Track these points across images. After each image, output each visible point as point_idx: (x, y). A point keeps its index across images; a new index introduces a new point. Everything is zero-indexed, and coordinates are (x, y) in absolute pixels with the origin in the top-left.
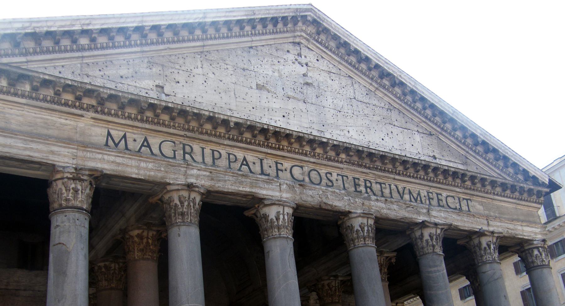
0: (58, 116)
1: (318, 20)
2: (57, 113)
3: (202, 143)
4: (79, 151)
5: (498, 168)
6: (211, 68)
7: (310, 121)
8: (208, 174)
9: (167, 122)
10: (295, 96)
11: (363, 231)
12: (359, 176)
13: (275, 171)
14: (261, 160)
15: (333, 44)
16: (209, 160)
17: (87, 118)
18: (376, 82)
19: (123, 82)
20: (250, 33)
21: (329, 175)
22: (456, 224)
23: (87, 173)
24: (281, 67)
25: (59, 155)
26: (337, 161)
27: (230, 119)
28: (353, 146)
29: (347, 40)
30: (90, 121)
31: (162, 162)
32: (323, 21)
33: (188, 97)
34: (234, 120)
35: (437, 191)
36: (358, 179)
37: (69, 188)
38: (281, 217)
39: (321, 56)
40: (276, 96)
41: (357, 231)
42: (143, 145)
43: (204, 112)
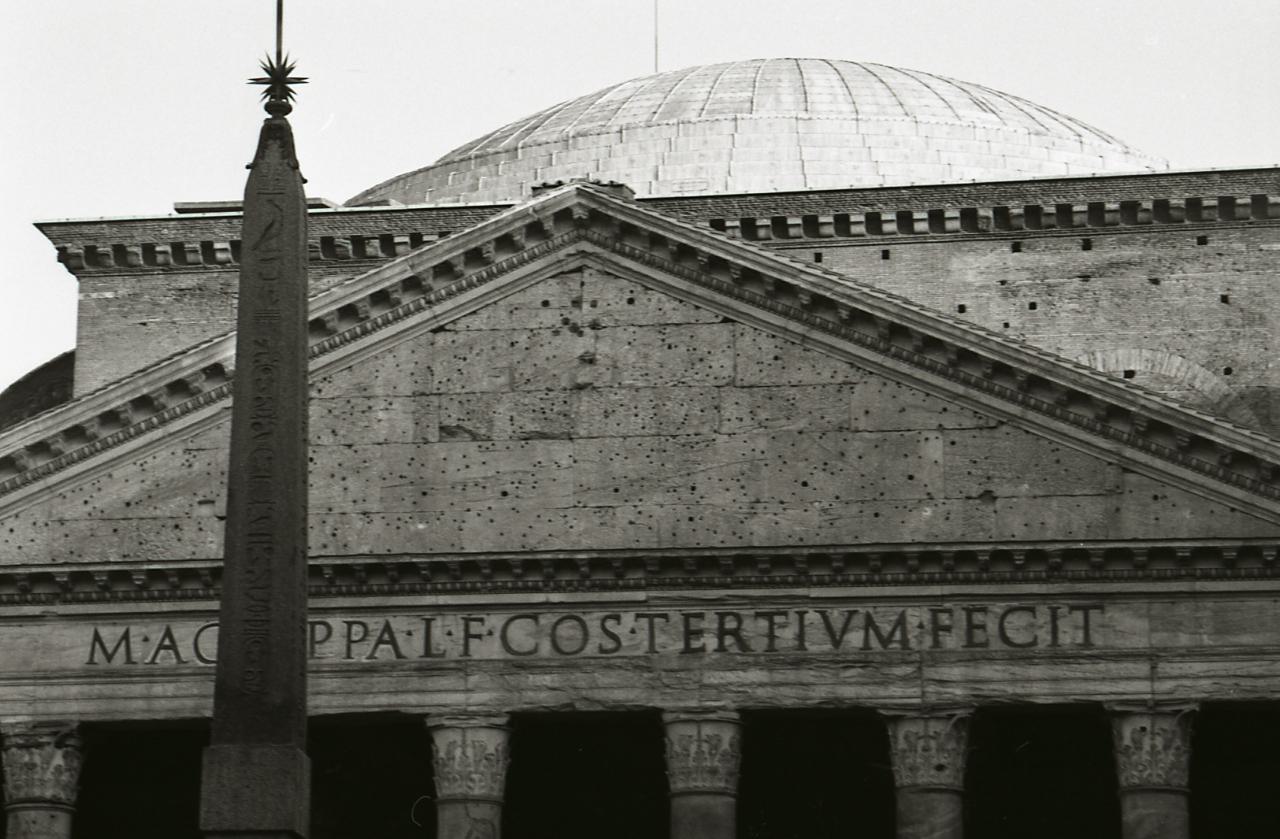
1: (602, 210)
4: (37, 688)
7: (578, 489)
10: (546, 430)
13: (462, 642)
15: (659, 254)
18: (798, 319)
19: (130, 516)
20: (423, 302)
21: (610, 624)
22: (1019, 690)
29: (684, 241)
36: (700, 616)
38: (458, 753)
39: (643, 286)
40: (489, 444)
42: (161, 647)
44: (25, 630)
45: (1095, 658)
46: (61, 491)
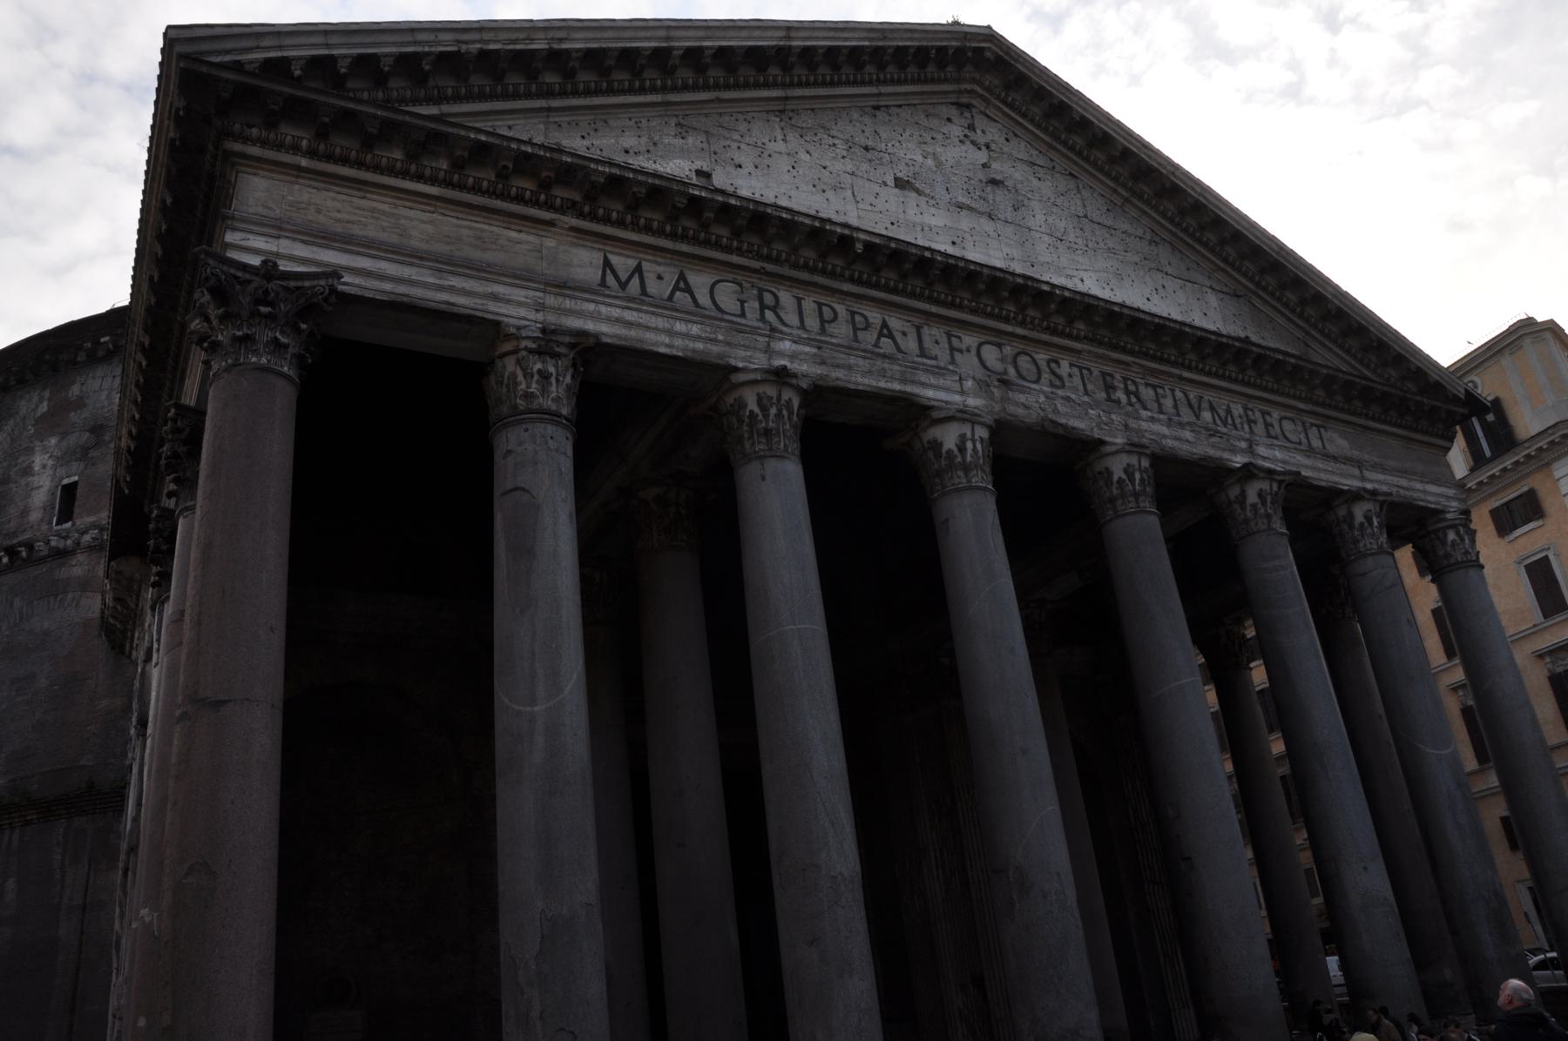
0: (502, 224)
1: (1007, 58)
2: (501, 218)
3: (798, 288)
4: (548, 296)
5: (1367, 367)
6: (803, 142)
8: (814, 350)
9: (725, 240)
10: (973, 205)
11: (1132, 480)
12: (1114, 369)
13: (948, 352)
14: (918, 329)
15: (1036, 111)
16: (812, 323)
17: (562, 228)
18: (1124, 186)
20: (875, 77)
21: (1053, 365)
23: (567, 339)
24: (939, 150)
25: (508, 302)
26: (1070, 337)
27: (855, 235)
28: (1102, 304)
29: (1064, 99)
30: (568, 236)
31: (718, 323)
32: (1016, 61)
33: (762, 195)
34: (862, 236)
35: (1260, 407)
36: (1111, 376)
37: (532, 369)
38: (969, 445)
39: (1013, 132)
40: (932, 202)
41: (1120, 481)
42: (676, 288)
43: (801, 219)
44: (523, 236)
45: (1335, 458)
46: (557, 119)
